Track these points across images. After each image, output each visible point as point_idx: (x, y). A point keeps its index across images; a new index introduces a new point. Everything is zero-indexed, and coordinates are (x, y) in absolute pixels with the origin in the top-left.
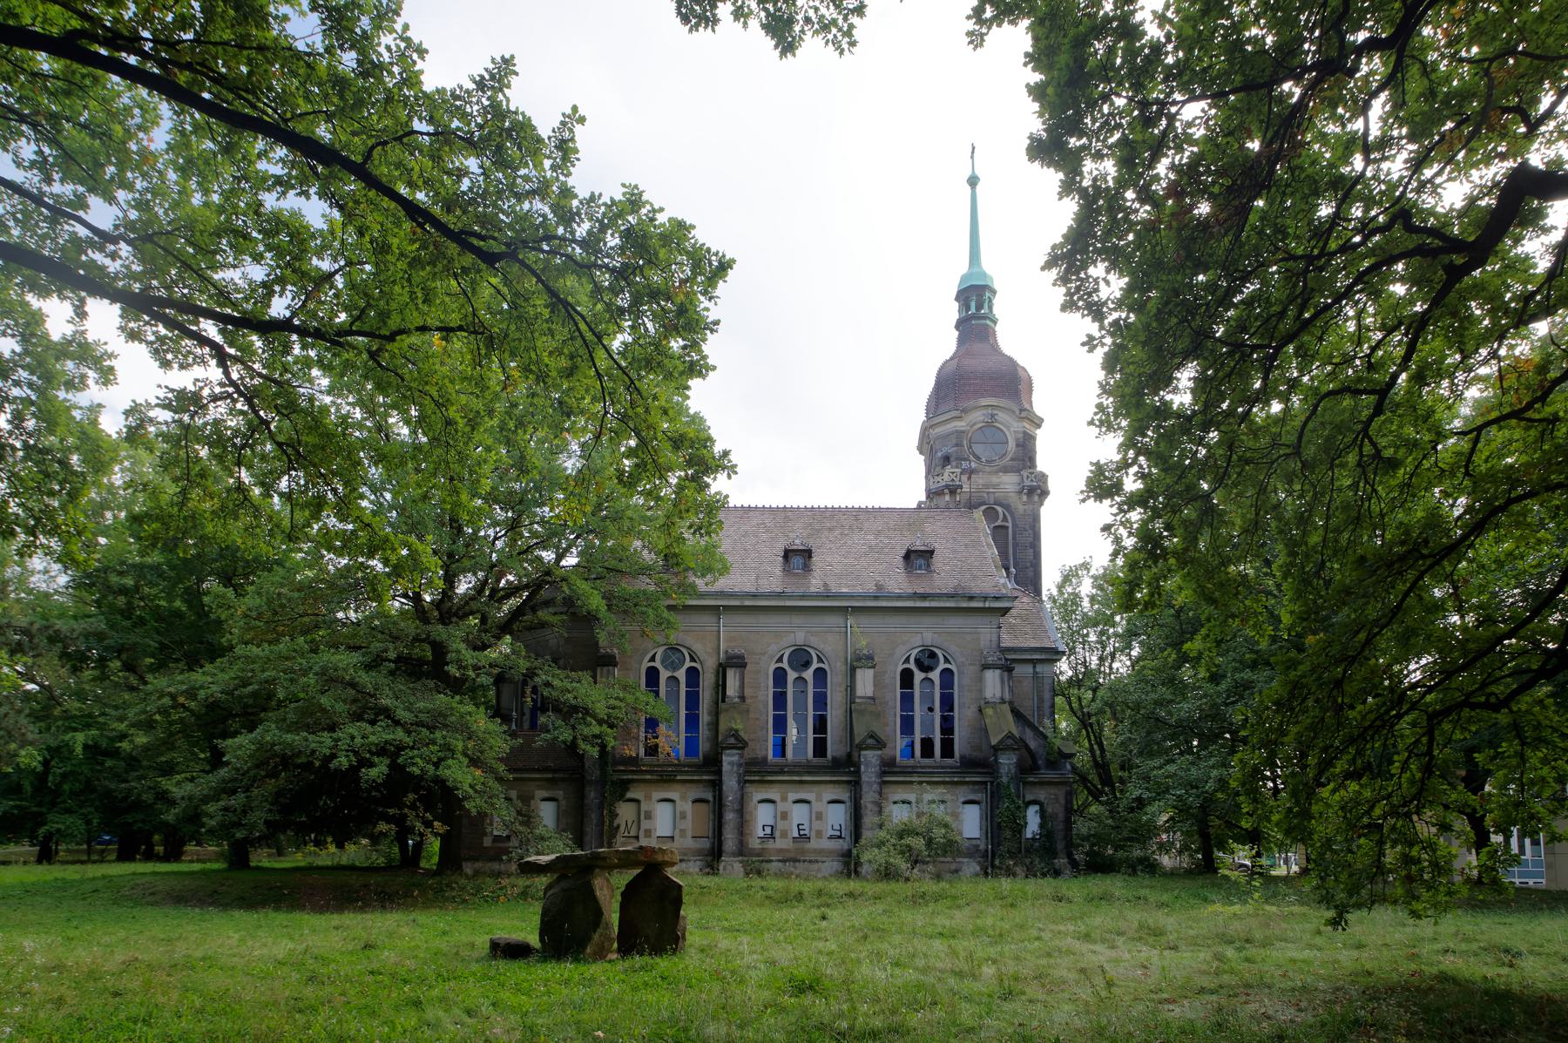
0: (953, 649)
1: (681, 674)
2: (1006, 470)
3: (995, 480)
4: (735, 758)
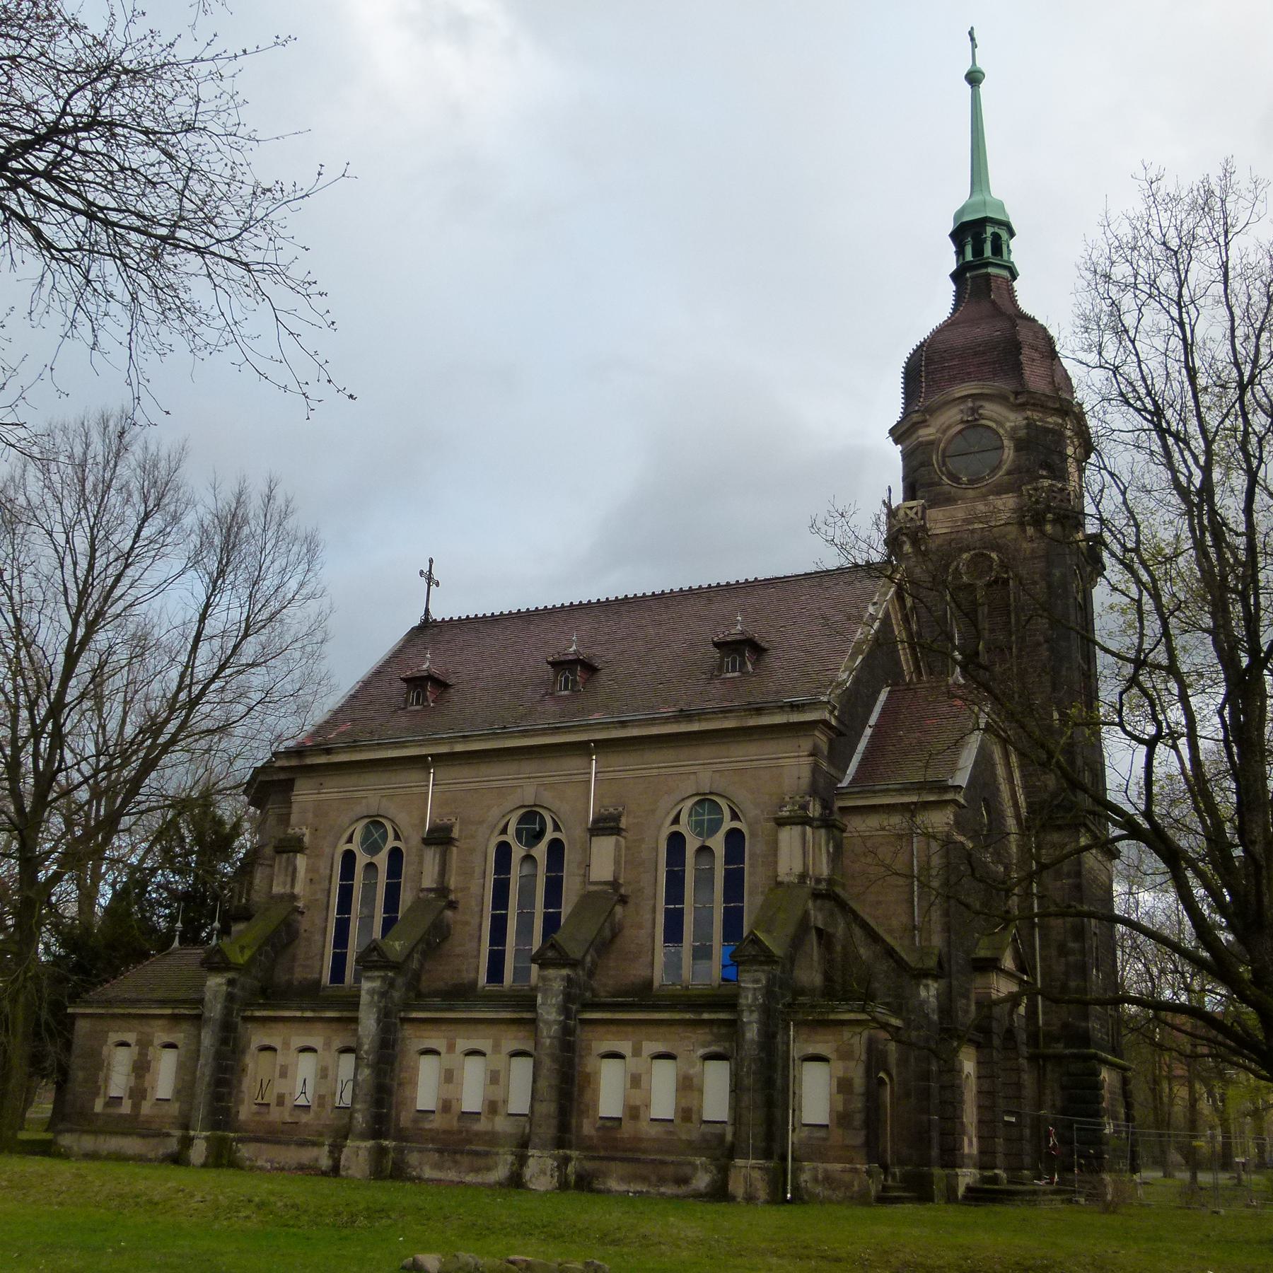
0: (744, 798)
2: (999, 490)
4: (377, 984)
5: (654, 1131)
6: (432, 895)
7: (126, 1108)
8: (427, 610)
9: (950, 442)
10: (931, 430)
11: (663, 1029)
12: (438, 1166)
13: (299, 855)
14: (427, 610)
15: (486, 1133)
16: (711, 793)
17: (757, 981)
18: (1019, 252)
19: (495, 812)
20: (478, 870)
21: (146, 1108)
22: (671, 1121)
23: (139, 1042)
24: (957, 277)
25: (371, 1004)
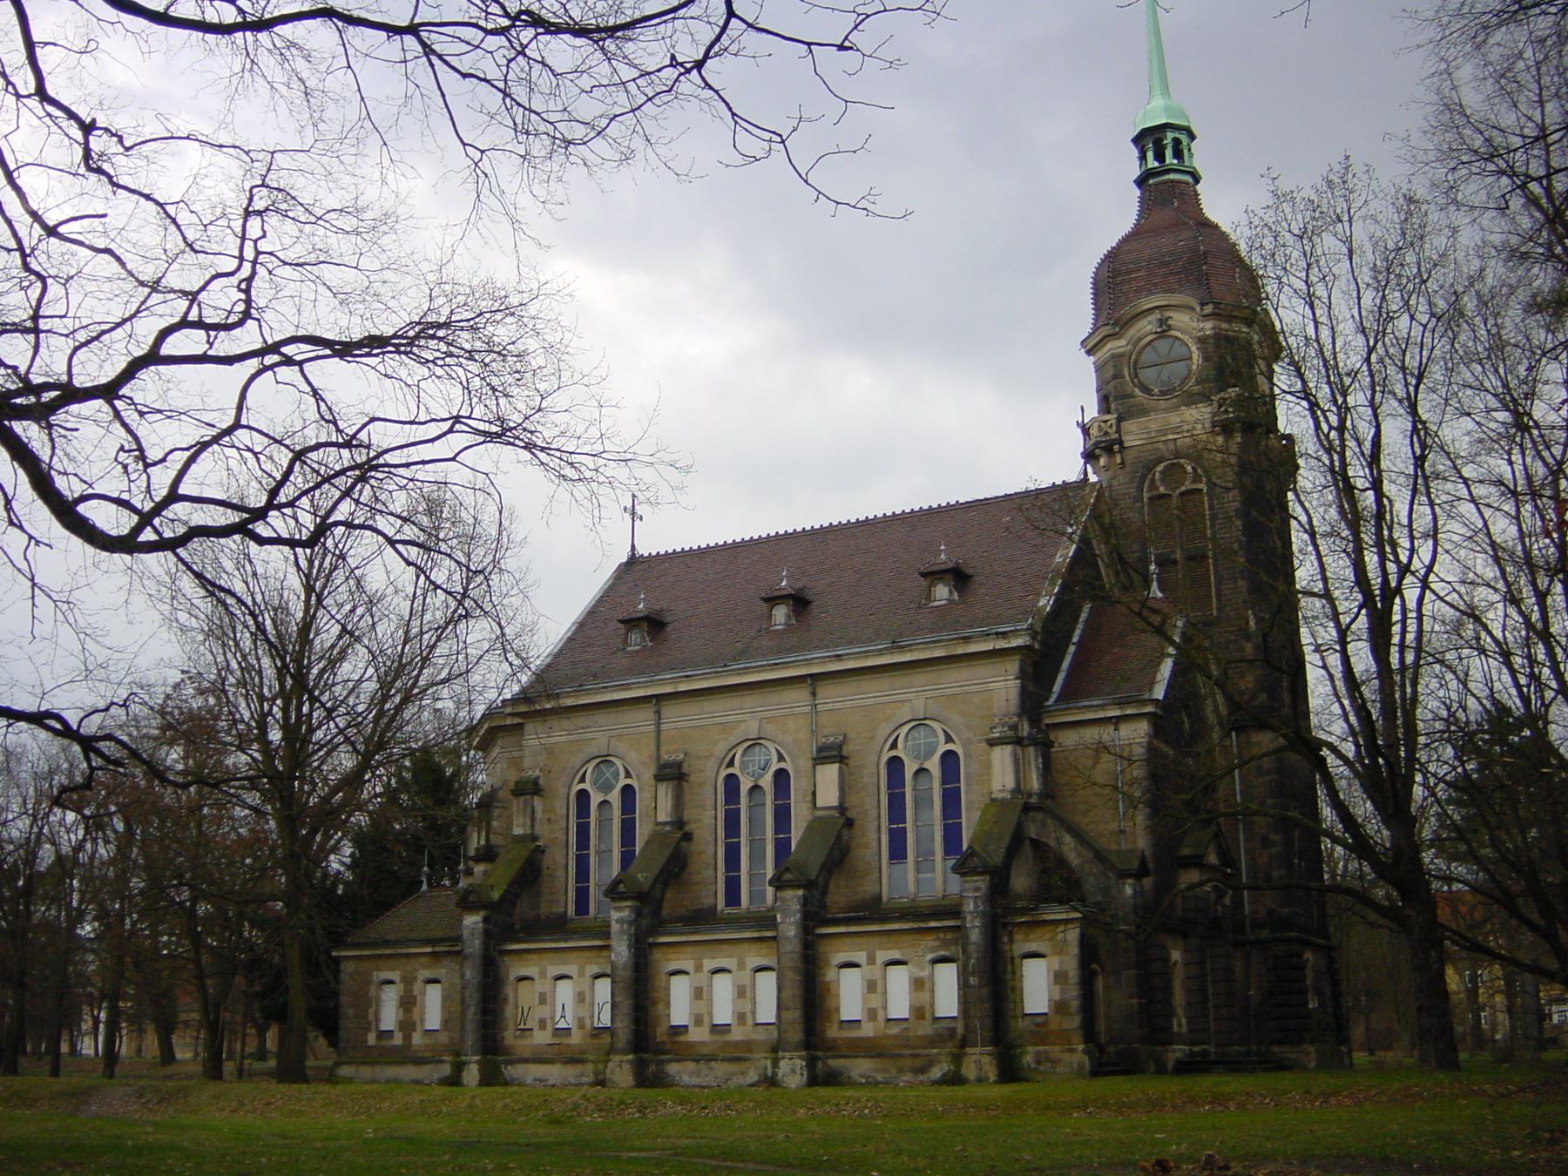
1: (615, 797)
3: (1174, 419)
4: (626, 913)
5: (894, 1030)
6: (667, 828)
7: (398, 1040)
8: (633, 546)
9: (1139, 354)
10: (1123, 342)
11: (895, 938)
14: (633, 546)
17: (977, 889)
18: (1200, 156)
20: (709, 802)
21: (417, 1039)
23: (404, 979)
24: (1141, 182)
25: (622, 932)
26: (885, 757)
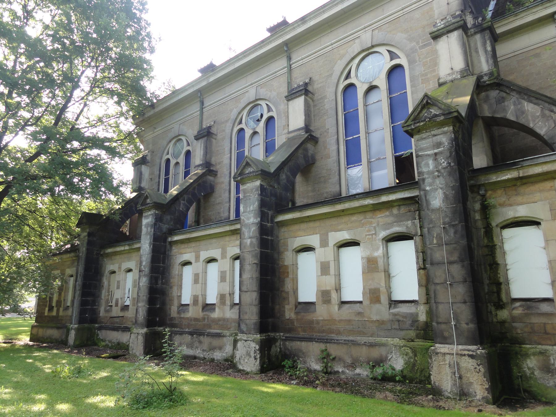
12: (190, 346)
13: (143, 166)
15: (219, 320)
16: (373, 47)
19: (235, 112)
20: (227, 149)
22: (361, 302)
25: (147, 233)
26: (341, 87)
